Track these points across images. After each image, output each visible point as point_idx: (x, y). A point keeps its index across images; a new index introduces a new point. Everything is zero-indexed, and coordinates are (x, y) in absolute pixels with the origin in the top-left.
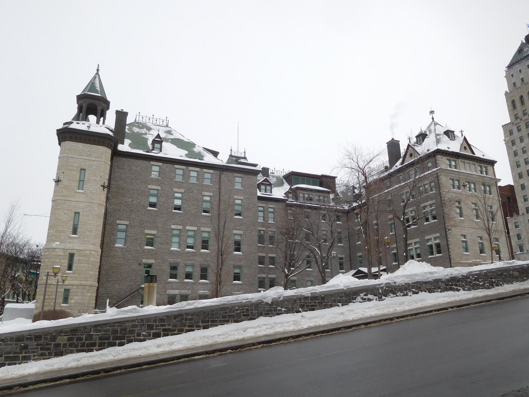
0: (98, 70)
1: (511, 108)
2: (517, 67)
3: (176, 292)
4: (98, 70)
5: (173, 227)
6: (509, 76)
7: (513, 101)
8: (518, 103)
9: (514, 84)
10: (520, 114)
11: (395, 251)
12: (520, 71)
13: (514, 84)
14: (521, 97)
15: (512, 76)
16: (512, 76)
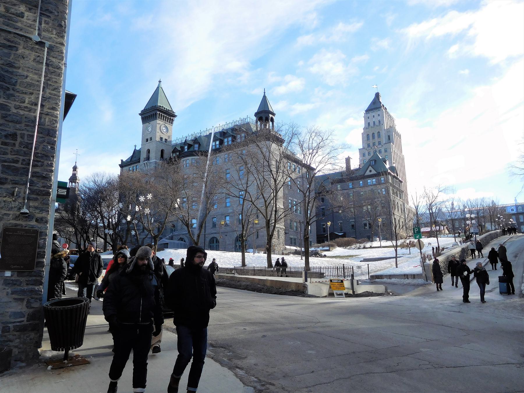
0: (265, 93)
1: (366, 139)
2: (371, 114)
3: (292, 237)
4: (265, 93)
5: (290, 198)
6: (366, 118)
7: (368, 135)
8: (371, 137)
9: (369, 124)
10: (371, 145)
11: (353, 223)
12: (374, 116)
13: (369, 124)
14: (373, 134)
15: (368, 118)
16: (368, 118)
